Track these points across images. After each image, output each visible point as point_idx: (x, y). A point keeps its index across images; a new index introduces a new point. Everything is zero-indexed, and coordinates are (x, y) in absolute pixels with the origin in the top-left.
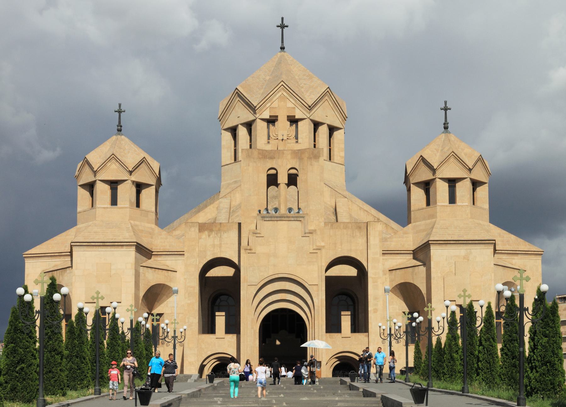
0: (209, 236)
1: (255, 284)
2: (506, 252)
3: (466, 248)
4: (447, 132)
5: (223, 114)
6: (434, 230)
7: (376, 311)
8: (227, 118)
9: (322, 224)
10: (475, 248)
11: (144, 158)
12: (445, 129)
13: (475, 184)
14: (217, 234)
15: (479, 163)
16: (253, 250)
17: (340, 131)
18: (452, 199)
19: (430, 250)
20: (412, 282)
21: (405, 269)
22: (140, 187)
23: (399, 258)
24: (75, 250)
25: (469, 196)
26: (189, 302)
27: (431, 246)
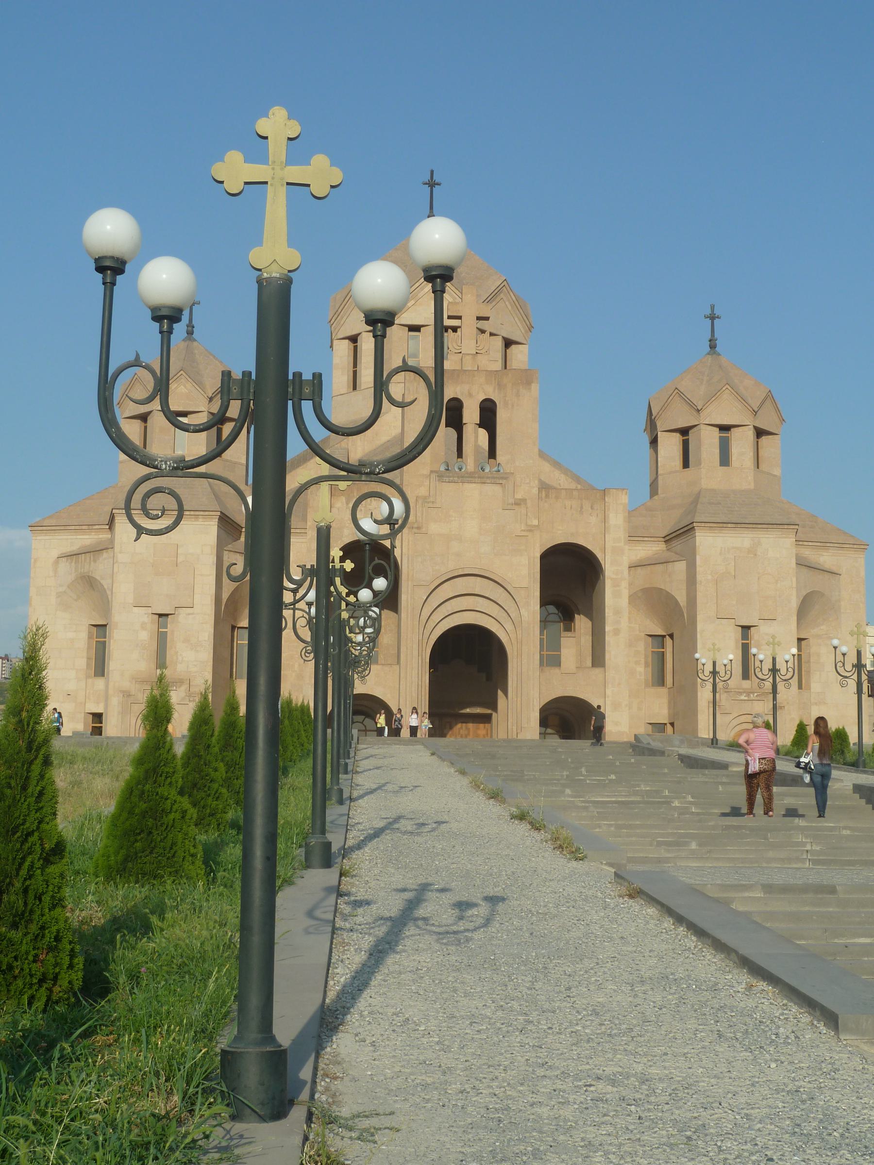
1: (424, 583)
2: (810, 544)
4: (714, 353)
5: (336, 316)
6: (699, 506)
7: (617, 632)
8: (342, 322)
9: (535, 491)
10: (767, 536)
13: (760, 433)
15: (768, 403)
17: (520, 346)
18: (725, 459)
20: (663, 588)
21: (649, 567)
23: (640, 548)
24: (121, 521)
25: (752, 454)
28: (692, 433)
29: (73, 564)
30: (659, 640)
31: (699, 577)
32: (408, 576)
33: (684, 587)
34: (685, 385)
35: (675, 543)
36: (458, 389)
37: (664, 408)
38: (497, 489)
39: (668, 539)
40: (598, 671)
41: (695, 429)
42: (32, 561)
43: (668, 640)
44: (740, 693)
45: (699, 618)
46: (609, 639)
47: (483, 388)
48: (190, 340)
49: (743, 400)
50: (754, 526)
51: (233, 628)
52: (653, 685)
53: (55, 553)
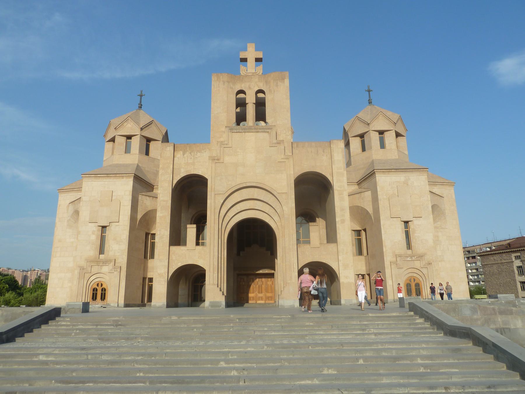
0: (183, 155)
1: (222, 193)
3: (405, 175)
6: (375, 164)
7: (343, 221)
10: (412, 175)
11: (153, 121)
12: (369, 103)
13: (398, 135)
14: (190, 153)
16: (221, 160)
19: (376, 177)
22: (149, 140)
24: (85, 181)
26: (161, 215)
27: (376, 174)
28: (365, 136)
29: (73, 206)
30: (358, 232)
31: (380, 197)
32: (211, 189)
33: (371, 203)
34: (361, 115)
35: (363, 184)
36: (243, 85)
37: (351, 127)
38: (266, 135)
39: (359, 183)
40: (332, 246)
41: (367, 133)
42: (58, 206)
43: (363, 233)
44: (407, 257)
45: (382, 218)
46: (339, 226)
47: (257, 84)
48: (139, 109)
49: (389, 119)
50: (406, 170)
51: (147, 234)
52: (356, 255)
53: (68, 202)
